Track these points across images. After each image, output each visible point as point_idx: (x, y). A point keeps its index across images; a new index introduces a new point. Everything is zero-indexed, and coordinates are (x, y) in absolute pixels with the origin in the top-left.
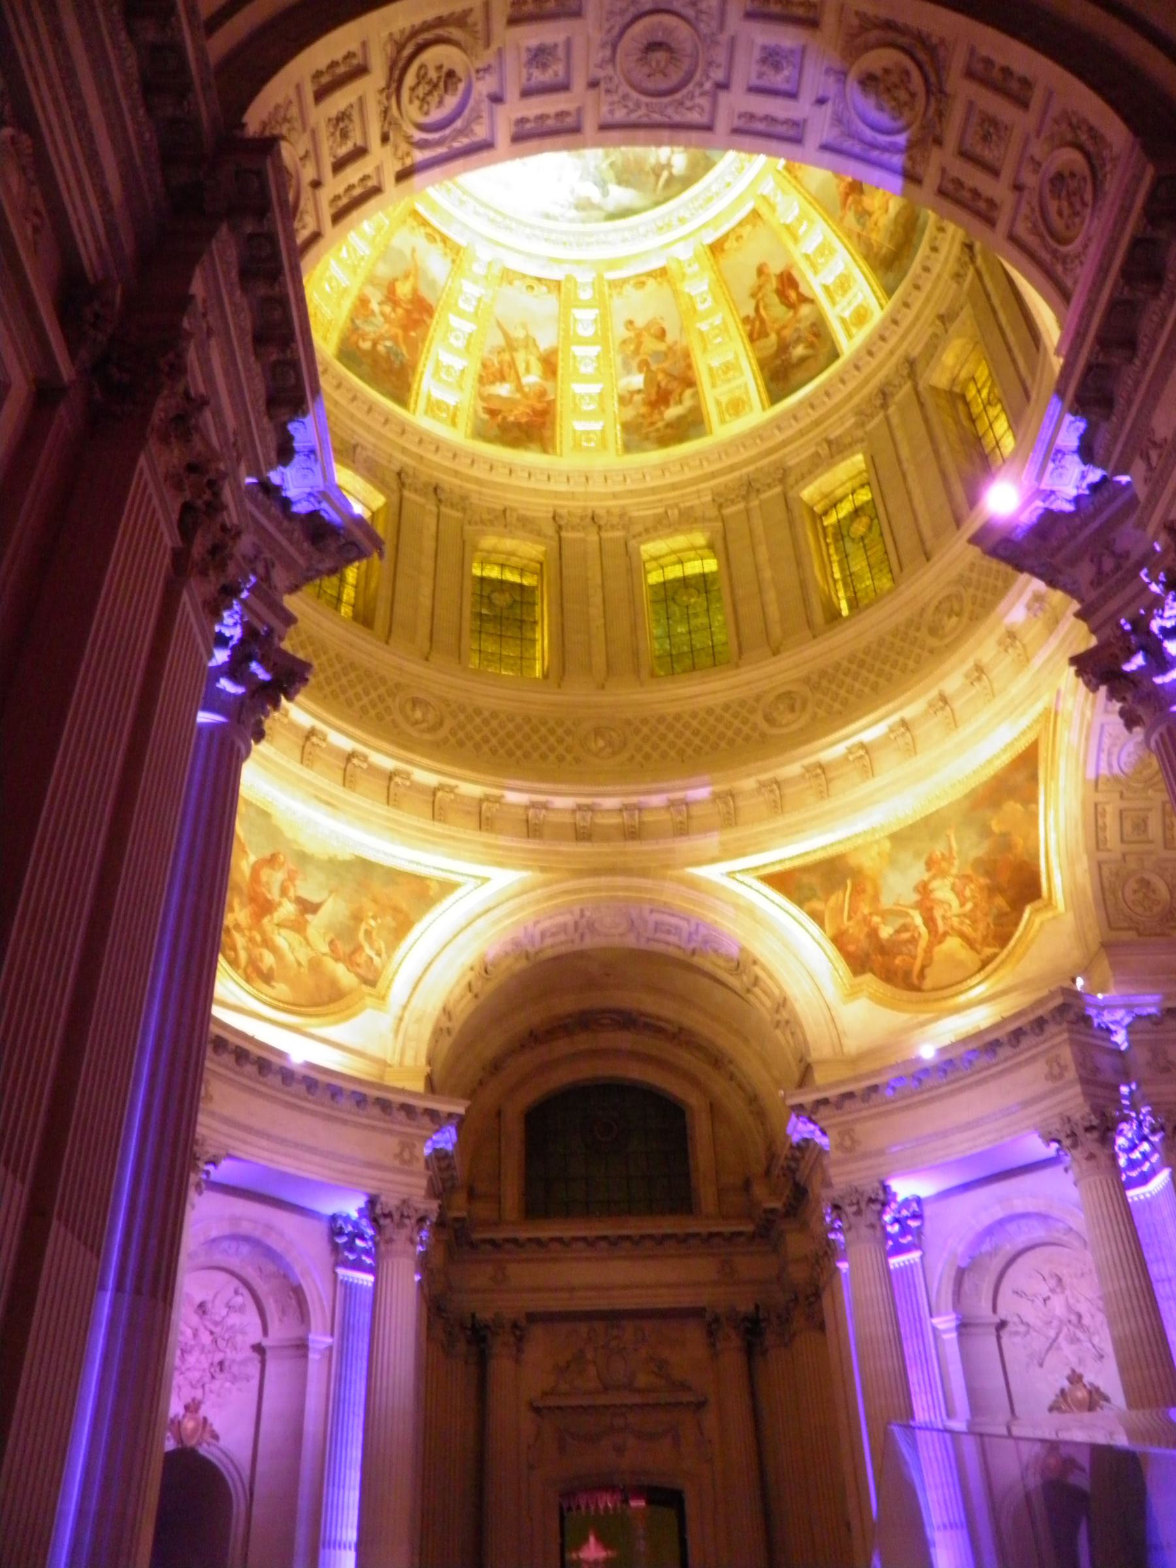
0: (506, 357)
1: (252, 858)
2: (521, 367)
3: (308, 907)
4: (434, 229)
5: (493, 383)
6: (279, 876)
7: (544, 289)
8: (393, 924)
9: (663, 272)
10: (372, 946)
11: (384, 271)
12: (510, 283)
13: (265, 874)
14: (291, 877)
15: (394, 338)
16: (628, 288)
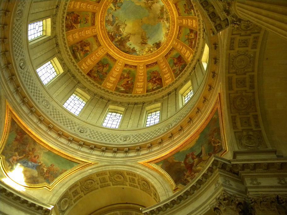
0: (190, 40)
1: (183, 162)
2: (191, 37)
3: (199, 156)
4: (169, 52)
5: (192, 44)
6: (190, 157)
7: (181, 30)
8: (216, 133)
9: (176, 4)
10: (217, 144)
11: (172, 65)
12: (179, 37)
13: (187, 162)
14: (193, 154)
15: (181, 65)
16: (180, 12)
